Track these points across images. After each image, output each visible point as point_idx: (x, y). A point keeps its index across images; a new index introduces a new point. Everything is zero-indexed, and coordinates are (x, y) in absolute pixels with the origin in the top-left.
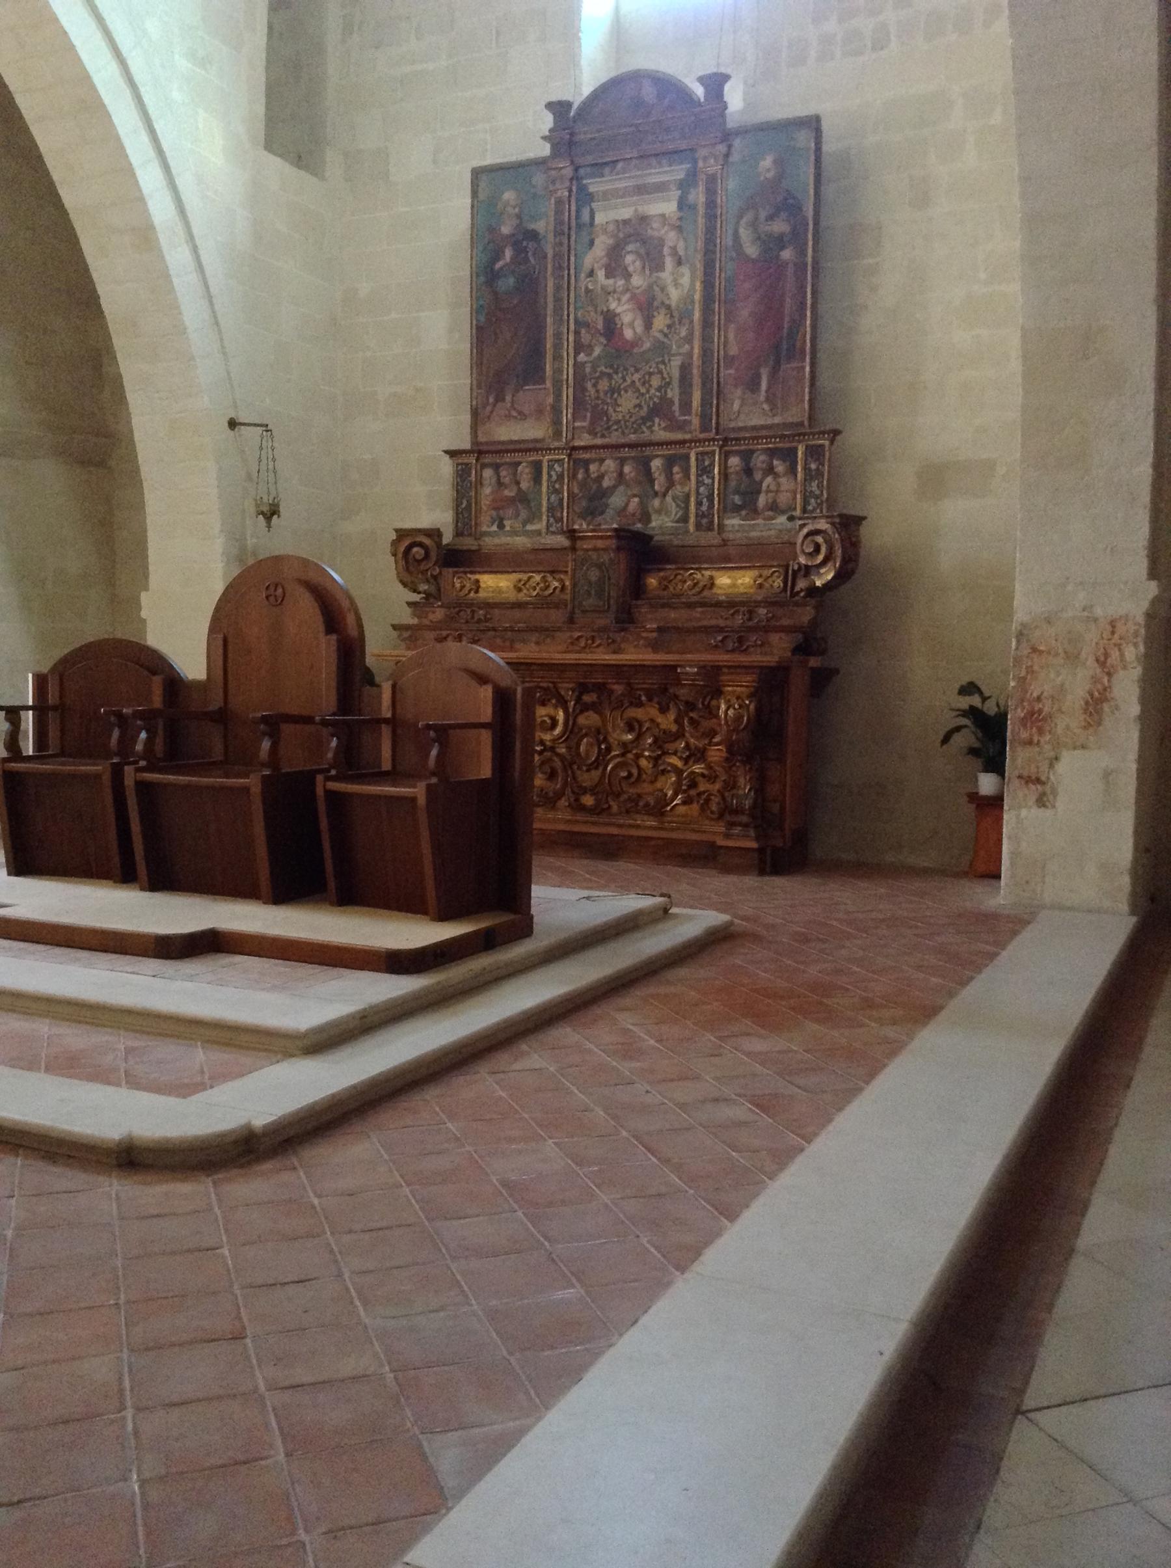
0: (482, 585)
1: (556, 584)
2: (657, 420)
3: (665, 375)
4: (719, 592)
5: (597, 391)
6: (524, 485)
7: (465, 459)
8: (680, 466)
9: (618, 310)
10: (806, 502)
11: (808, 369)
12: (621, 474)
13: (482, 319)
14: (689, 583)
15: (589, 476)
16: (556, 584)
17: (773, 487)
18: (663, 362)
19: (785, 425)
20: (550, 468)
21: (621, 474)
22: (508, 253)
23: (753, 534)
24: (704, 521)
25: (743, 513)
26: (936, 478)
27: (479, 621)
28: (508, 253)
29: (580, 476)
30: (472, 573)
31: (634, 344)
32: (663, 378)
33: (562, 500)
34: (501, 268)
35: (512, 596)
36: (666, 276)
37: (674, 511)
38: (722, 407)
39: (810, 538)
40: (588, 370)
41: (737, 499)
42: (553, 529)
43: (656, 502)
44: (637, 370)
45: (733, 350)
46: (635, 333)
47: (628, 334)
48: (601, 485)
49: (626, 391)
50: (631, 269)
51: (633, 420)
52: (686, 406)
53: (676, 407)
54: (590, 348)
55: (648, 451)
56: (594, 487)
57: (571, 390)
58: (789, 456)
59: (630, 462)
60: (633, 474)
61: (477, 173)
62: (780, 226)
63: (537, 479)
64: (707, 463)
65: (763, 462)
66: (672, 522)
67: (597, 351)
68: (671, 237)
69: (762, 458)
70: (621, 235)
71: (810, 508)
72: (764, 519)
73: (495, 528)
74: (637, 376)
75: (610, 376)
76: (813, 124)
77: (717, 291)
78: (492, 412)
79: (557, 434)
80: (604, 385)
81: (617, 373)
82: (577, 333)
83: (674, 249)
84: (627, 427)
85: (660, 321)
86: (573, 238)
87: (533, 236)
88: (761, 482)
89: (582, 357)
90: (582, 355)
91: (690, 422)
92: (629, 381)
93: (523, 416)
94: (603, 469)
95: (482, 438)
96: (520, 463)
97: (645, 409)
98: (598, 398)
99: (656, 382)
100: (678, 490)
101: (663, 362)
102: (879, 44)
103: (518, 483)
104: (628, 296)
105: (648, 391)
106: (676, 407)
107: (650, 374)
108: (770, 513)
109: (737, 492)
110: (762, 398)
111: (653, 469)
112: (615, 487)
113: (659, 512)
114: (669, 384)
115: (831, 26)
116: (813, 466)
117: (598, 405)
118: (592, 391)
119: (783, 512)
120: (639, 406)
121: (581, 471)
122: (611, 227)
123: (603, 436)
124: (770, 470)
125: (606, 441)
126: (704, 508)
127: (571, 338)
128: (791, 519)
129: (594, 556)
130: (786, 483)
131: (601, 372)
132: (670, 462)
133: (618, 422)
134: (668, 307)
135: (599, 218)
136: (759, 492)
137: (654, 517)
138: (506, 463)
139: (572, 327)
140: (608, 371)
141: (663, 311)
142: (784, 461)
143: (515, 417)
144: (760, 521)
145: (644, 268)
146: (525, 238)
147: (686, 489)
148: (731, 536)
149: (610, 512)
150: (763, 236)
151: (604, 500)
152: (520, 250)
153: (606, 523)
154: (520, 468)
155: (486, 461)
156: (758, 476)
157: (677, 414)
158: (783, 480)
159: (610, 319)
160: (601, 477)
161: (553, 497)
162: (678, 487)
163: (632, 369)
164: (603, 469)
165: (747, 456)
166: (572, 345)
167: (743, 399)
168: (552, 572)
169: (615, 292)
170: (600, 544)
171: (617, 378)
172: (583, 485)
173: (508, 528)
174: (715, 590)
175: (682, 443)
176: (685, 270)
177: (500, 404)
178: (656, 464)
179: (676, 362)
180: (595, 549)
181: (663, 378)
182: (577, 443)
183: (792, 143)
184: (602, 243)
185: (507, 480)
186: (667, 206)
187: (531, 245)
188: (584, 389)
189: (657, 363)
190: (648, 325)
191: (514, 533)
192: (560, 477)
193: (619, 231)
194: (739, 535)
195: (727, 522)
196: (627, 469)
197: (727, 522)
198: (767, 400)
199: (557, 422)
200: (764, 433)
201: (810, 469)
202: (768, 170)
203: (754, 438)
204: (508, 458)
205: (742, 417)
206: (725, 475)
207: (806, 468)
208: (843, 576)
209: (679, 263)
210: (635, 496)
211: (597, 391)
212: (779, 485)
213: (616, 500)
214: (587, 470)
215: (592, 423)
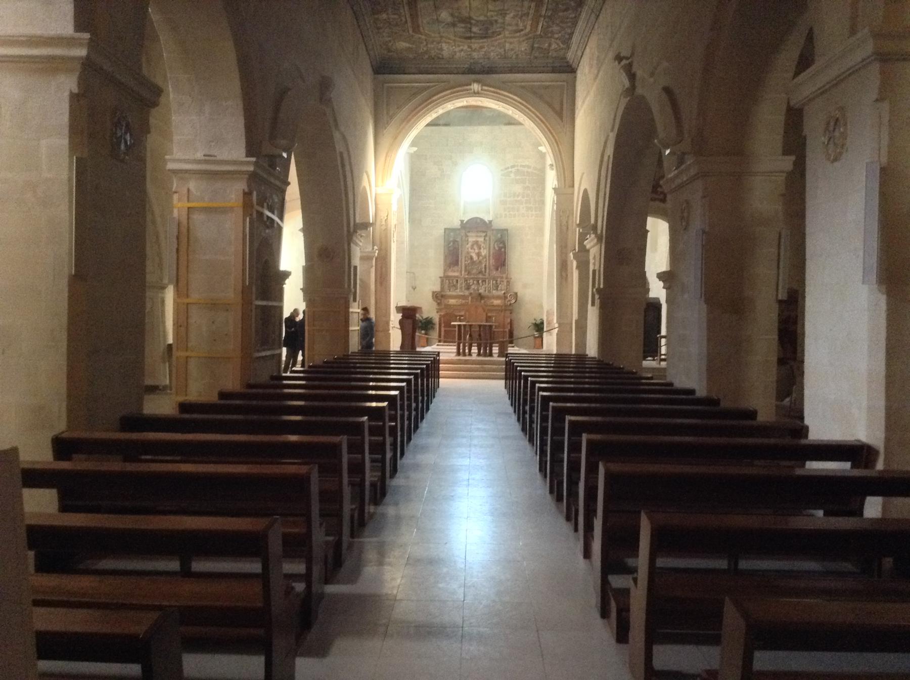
26: (525, 286)
76: (507, 230)
146: (455, 241)
184: (470, 244)
186: (482, 239)
213: (473, 287)
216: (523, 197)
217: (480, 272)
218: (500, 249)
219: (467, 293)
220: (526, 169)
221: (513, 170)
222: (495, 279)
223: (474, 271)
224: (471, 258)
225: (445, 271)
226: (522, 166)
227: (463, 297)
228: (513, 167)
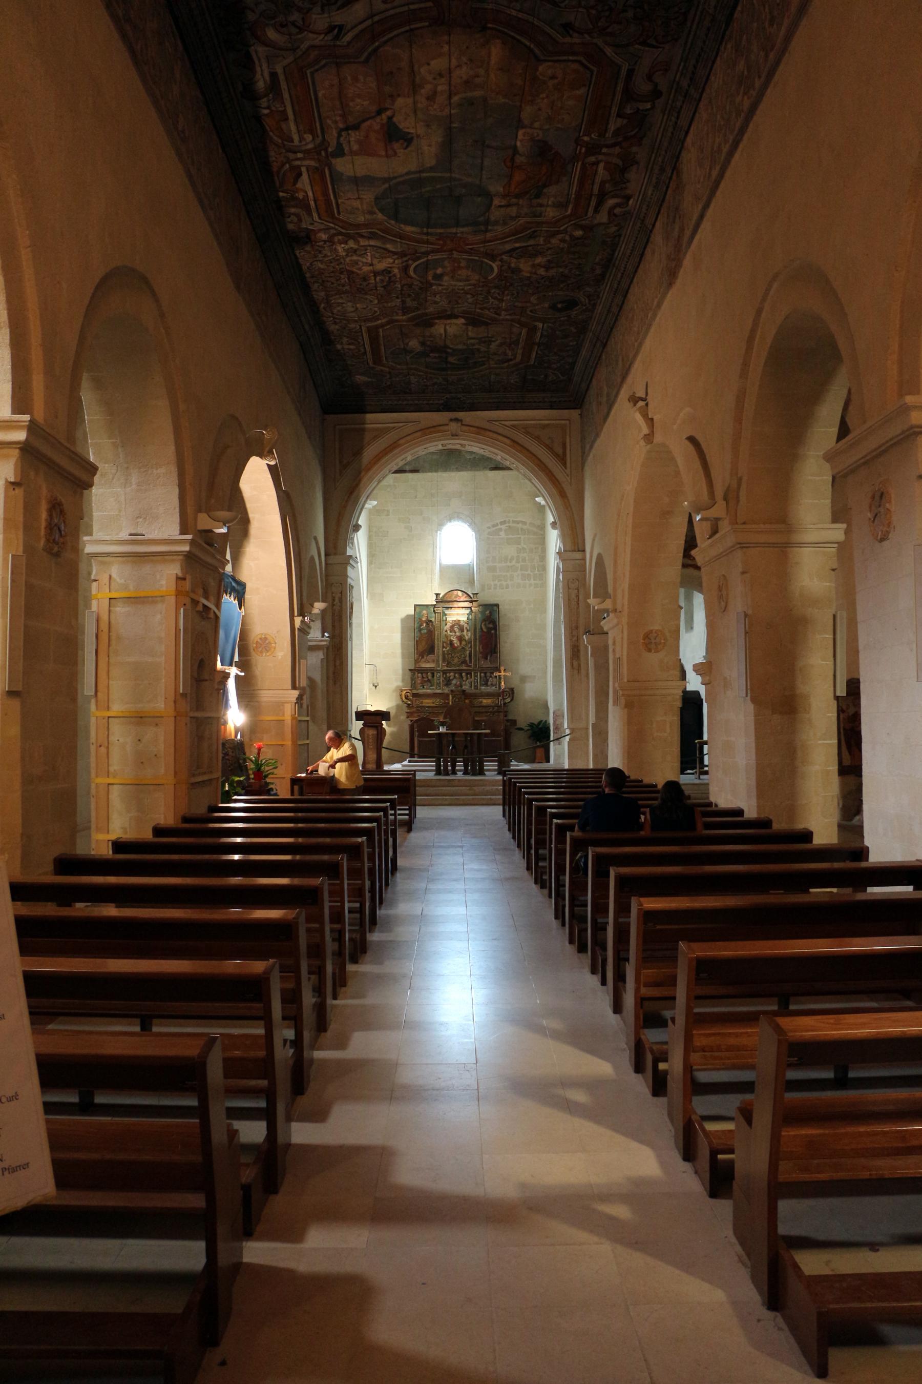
26: (524, 679)
36: (465, 633)
52: (470, 662)
61: (415, 606)
62: (491, 626)
63: (433, 676)
68: (466, 625)
76: (497, 605)
85: (464, 643)
93: (429, 662)
102: (507, 587)
115: (496, 582)
132: (467, 674)
152: (427, 623)
159: (451, 641)
165: (485, 673)
184: (449, 625)
208: (512, 700)
213: (454, 682)
216: (518, 562)
217: (464, 662)
218: (489, 629)
219: (446, 690)
220: (520, 526)
221: (503, 527)
222: (483, 670)
223: (456, 660)
224: (451, 643)
225: (416, 661)
226: (514, 522)
227: (445, 696)
228: (503, 523)
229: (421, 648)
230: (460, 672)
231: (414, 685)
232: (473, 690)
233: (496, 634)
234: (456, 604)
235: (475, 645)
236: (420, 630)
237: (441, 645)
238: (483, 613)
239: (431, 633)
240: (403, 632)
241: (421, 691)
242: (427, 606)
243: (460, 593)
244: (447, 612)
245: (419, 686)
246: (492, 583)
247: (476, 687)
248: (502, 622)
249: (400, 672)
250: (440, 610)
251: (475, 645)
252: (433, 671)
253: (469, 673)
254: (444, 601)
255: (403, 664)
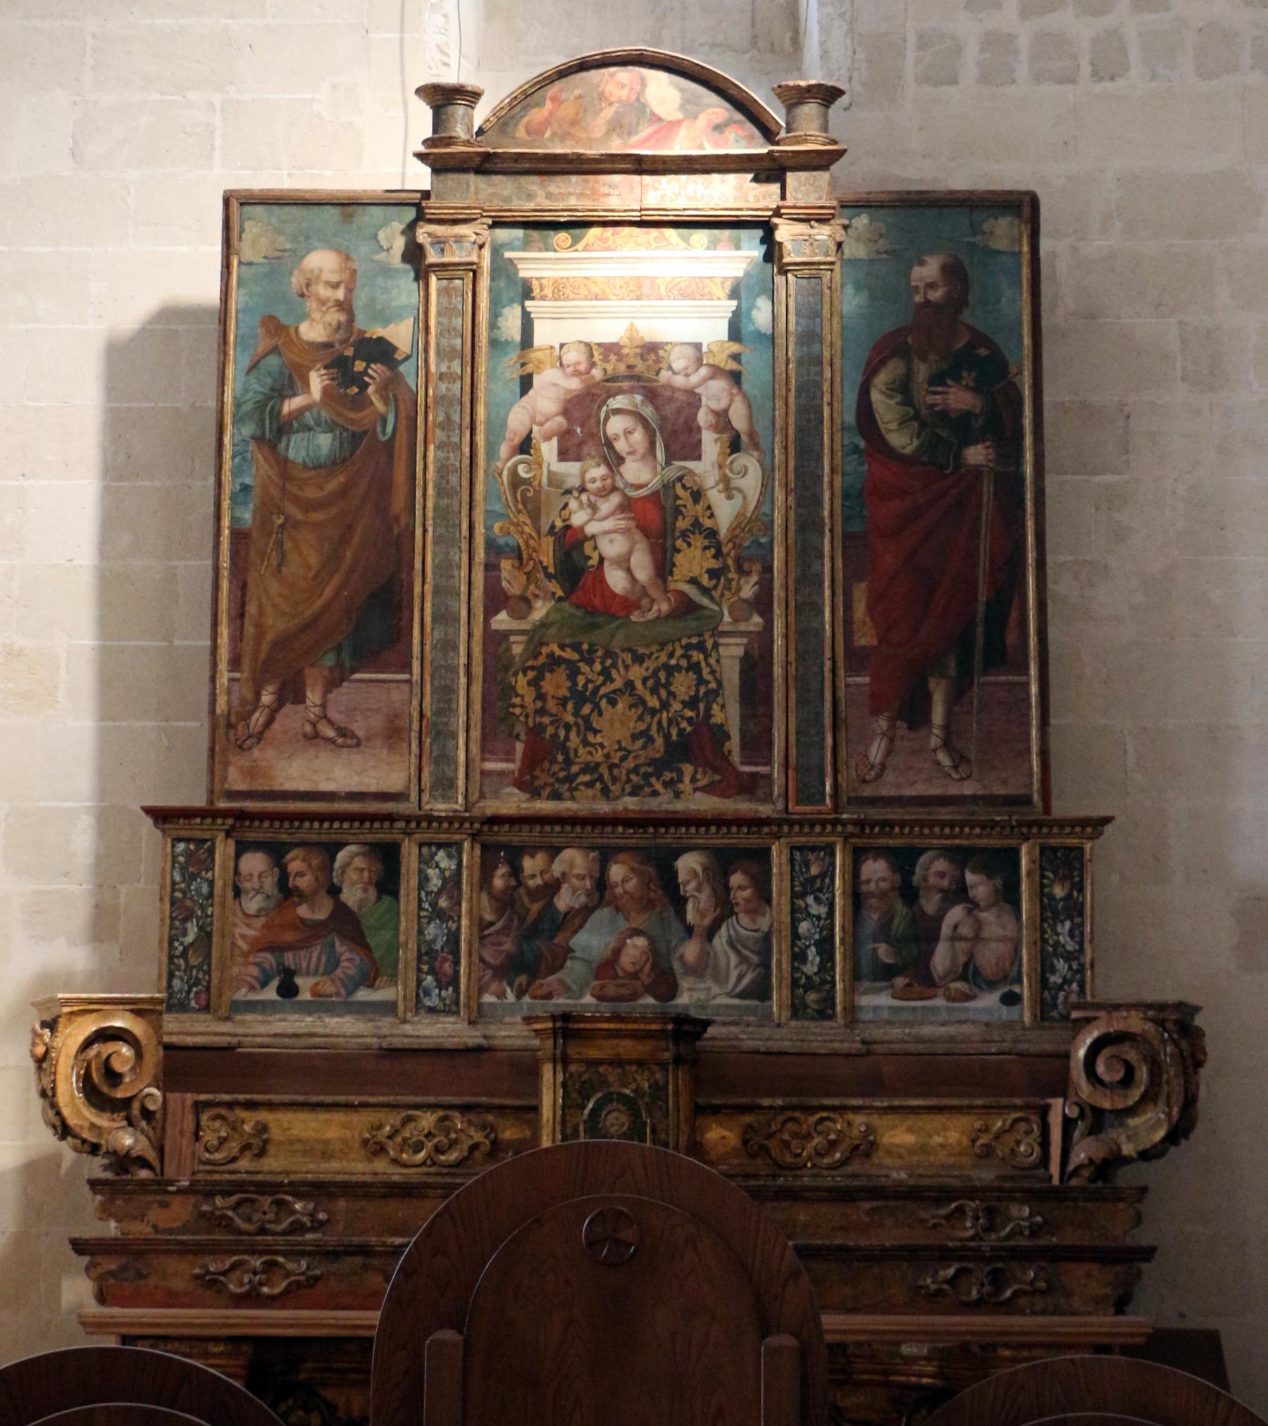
0: (275, 1133)
1: (478, 1136)
2: (688, 769)
3: (706, 674)
4: (888, 1161)
5: (541, 696)
6: (352, 896)
7: (198, 829)
8: (745, 873)
9: (591, 529)
10: (1046, 967)
11: (1034, 689)
12: (601, 885)
13: (247, 516)
14: (817, 1140)
15: (520, 883)
16: (478, 1136)
17: (966, 930)
18: (701, 647)
19: (991, 800)
20: (425, 861)
21: (601, 885)
22: (317, 381)
23: (928, 1031)
24: (812, 997)
25: (900, 981)
27: (297, 1228)
28: (317, 381)
29: (498, 882)
30: (251, 1106)
31: (628, 604)
32: (701, 681)
33: (454, 938)
34: (300, 412)
35: (359, 1168)
37: (736, 972)
38: (843, 753)
39: (1107, 1052)
40: (517, 650)
41: (883, 950)
42: (432, 1001)
43: (691, 950)
44: (639, 659)
45: (866, 638)
46: (633, 579)
47: (616, 580)
48: (550, 905)
49: (613, 703)
50: (621, 446)
51: (630, 763)
52: (757, 744)
53: (734, 745)
54: (524, 604)
55: (669, 838)
56: (535, 907)
57: (477, 689)
58: (1001, 863)
59: (622, 856)
60: (632, 885)
61: (237, 205)
62: (959, 398)
63: (388, 884)
64: (814, 870)
65: (942, 875)
66: (730, 994)
67: (541, 610)
68: (715, 394)
69: (941, 865)
70: (597, 373)
71: (1055, 979)
72: (950, 998)
73: (270, 994)
74: (636, 673)
75: (574, 673)
76: (1024, 207)
77: (826, 513)
78: (268, 724)
79: (445, 785)
80: (555, 684)
81: (590, 663)
82: (491, 567)
83: (722, 420)
84: (615, 780)
85: (692, 561)
86: (482, 369)
87: (382, 351)
88: (940, 917)
89: (502, 620)
90: (503, 615)
91: (769, 777)
92: (619, 683)
93: (347, 739)
94: (557, 868)
95: (237, 782)
96: (341, 845)
97: (659, 741)
98: (541, 712)
99: (683, 685)
100: (742, 925)
101: (701, 647)
102: (1108, 66)
103: (335, 891)
104: (615, 499)
105: (665, 705)
106: (734, 745)
107: (670, 670)
108: (959, 985)
109: (884, 931)
110: (934, 741)
111: (682, 877)
112: (584, 913)
113: (697, 971)
114: (716, 693)
115: (1007, 18)
116: (1059, 891)
117: (540, 728)
118: (528, 695)
119: (992, 985)
120: (645, 734)
121: (502, 870)
122: (573, 356)
123: (556, 796)
124: (959, 893)
125: (566, 806)
126: (811, 968)
127: (479, 577)
128: (1011, 999)
129: (612, 1074)
130: (995, 923)
131: (551, 655)
132: (722, 864)
133: (589, 768)
134: (712, 534)
135: (544, 334)
136: (934, 937)
137: (684, 983)
138: (302, 844)
139: (480, 555)
140: (570, 654)
141: (698, 541)
142: (990, 876)
143: (331, 741)
144: (939, 1002)
145: (652, 445)
147: (764, 923)
148: (876, 1033)
149: (573, 970)
150: (924, 412)
151: (559, 940)
153: (567, 990)
154: (342, 856)
155: (251, 836)
156: (930, 904)
157: (736, 758)
158: (987, 916)
159: (572, 544)
160: (553, 887)
161: (431, 930)
162: (744, 919)
163: (628, 657)
164: (557, 868)
165: (903, 860)
166: (478, 593)
167: (891, 740)
168: (465, 1109)
169: (583, 489)
170: (627, 1048)
171: (589, 673)
172: (505, 903)
173: (305, 996)
174: (879, 1157)
175: (755, 823)
176: (749, 461)
177: (288, 709)
178: (689, 865)
179: (731, 652)
180: (617, 1062)
181: (701, 681)
182: (492, 807)
183: (978, 238)
185: (304, 883)
187: (377, 370)
188: (511, 690)
189: (688, 647)
190: (663, 568)
191: (321, 1005)
192: (452, 883)
193: (593, 365)
194: (895, 1032)
195: (865, 1001)
196: (617, 872)
197: (865, 1001)
198: (947, 745)
199: (444, 758)
200: (945, 814)
201: (1051, 897)
202: (931, 286)
203: (922, 824)
204: (312, 832)
205: (889, 776)
206: (857, 899)
207: (1042, 894)
208: (1178, 1133)
209: (735, 446)
210: (636, 932)
211: (541, 696)
212: (979, 926)
213: (591, 940)
214: (516, 871)
215: (534, 759)
217: (695, 746)
223: (616, 726)
224: (573, 562)
225: (230, 734)
229: (275, 611)
230: (655, 841)
231: (190, 967)
232: (778, 1029)
233: (1010, 487)
234: (622, 194)
235: (807, 579)
236: (273, 431)
237: (470, 583)
238: (885, 275)
239: (373, 466)
240: (119, 469)
241: (272, 1028)
242: (348, 204)
243: (662, 91)
244: (539, 264)
245: (241, 976)
246: (969, 28)
247: (813, 999)
248: (1068, 381)
249: (82, 841)
250: (466, 243)
251: (807, 579)
252: (381, 830)
253: (738, 854)
254: (501, 163)
255: (111, 757)
